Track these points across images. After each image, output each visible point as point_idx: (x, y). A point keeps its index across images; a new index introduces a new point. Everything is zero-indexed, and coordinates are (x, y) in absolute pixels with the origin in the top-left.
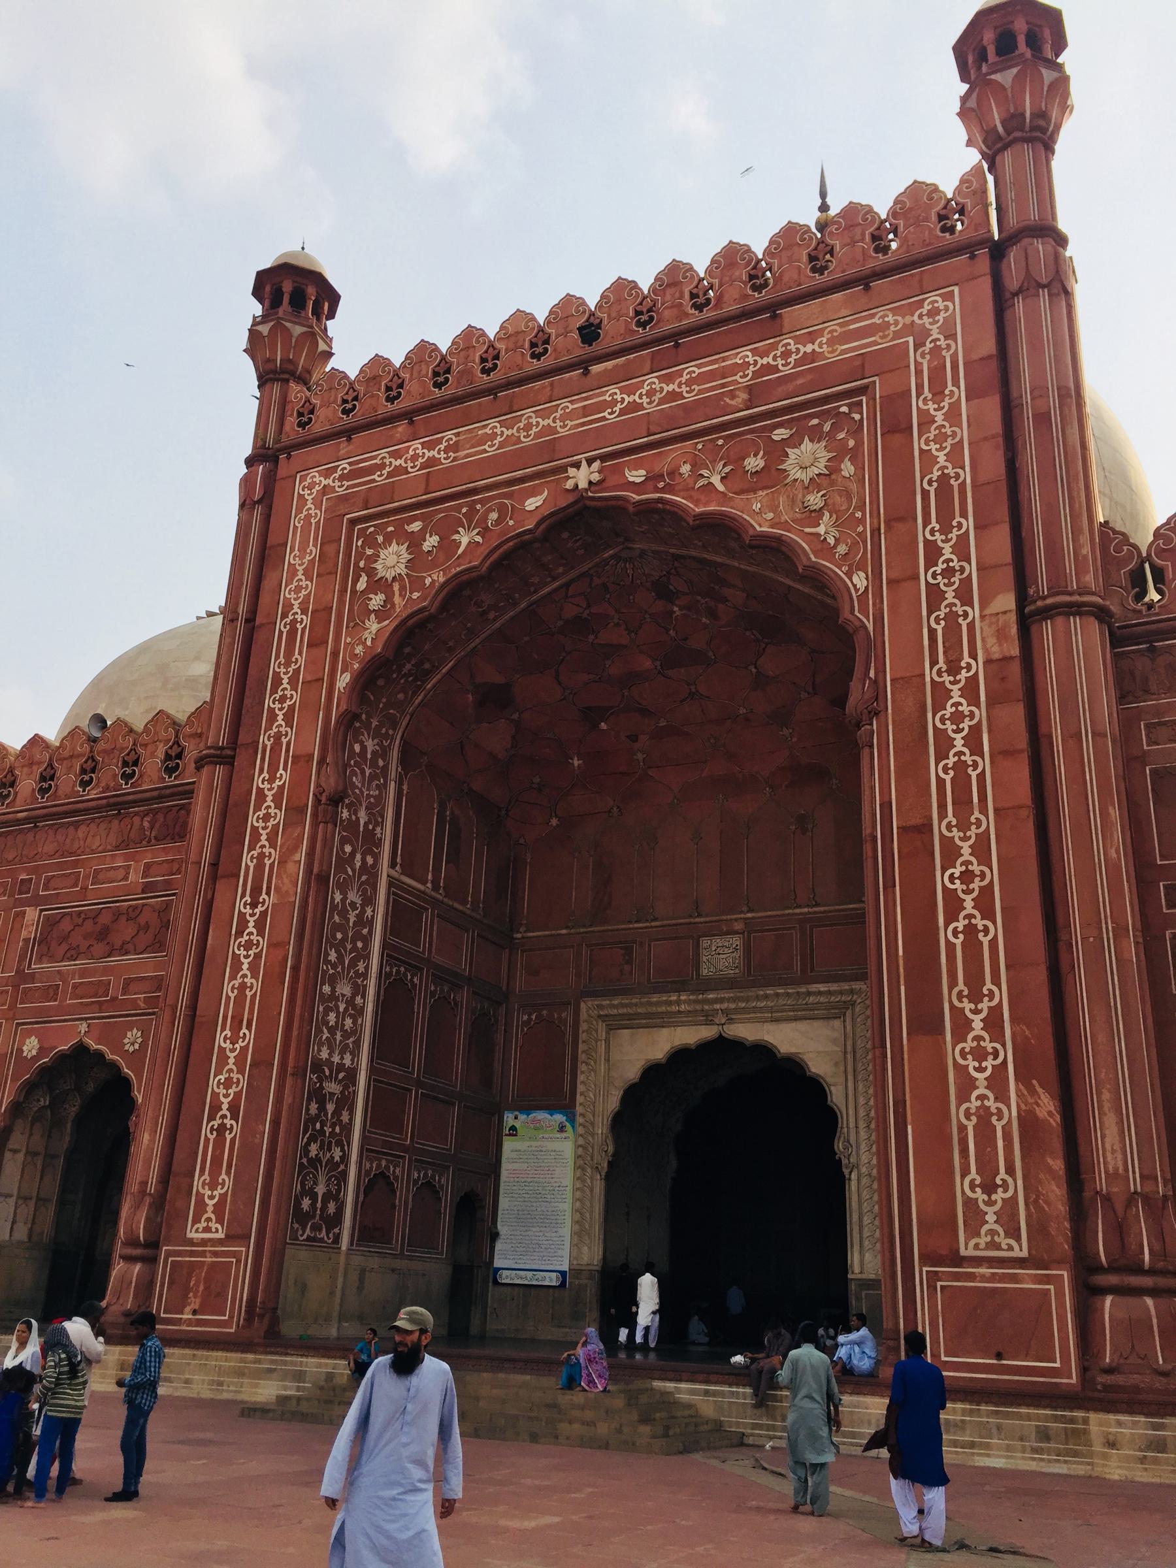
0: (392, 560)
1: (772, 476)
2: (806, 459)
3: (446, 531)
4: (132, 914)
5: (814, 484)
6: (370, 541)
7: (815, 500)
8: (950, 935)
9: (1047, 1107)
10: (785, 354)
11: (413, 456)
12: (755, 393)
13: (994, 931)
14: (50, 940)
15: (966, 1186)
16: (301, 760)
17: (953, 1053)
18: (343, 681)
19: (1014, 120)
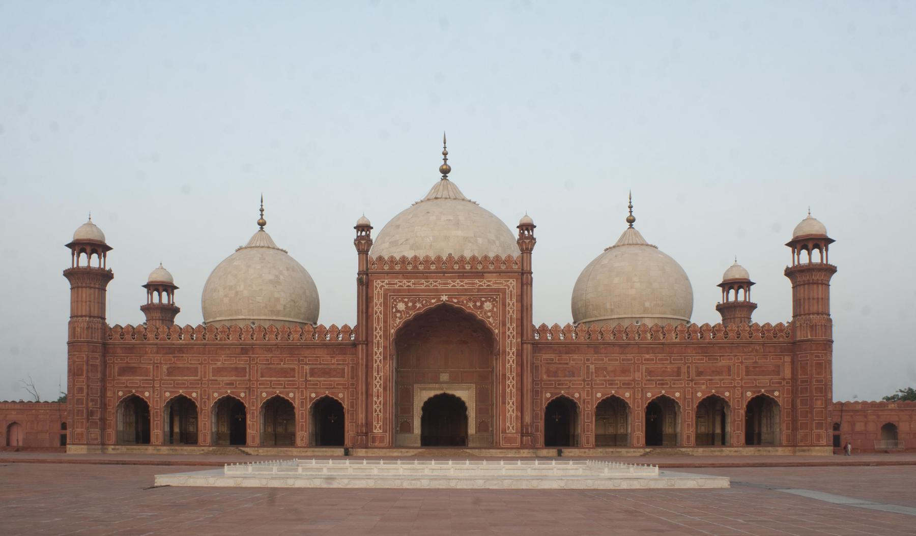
0: (401, 306)
1: (481, 307)
2: (488, 306)
3: (414, 303)
4: (335, 370)
5: (490, 311)
6: (395, 300)
7: (489, 314)
8: (508, 390)
9: (519, 414)
10: (483, 283)
11: (405, 283)
12: (479, 290)
13: (514, 390)
14: (313, 373)
15: (508, 424)
16: (385, 348)
17: (507, 407)
18: (392, 331)
19: (527, 249)
